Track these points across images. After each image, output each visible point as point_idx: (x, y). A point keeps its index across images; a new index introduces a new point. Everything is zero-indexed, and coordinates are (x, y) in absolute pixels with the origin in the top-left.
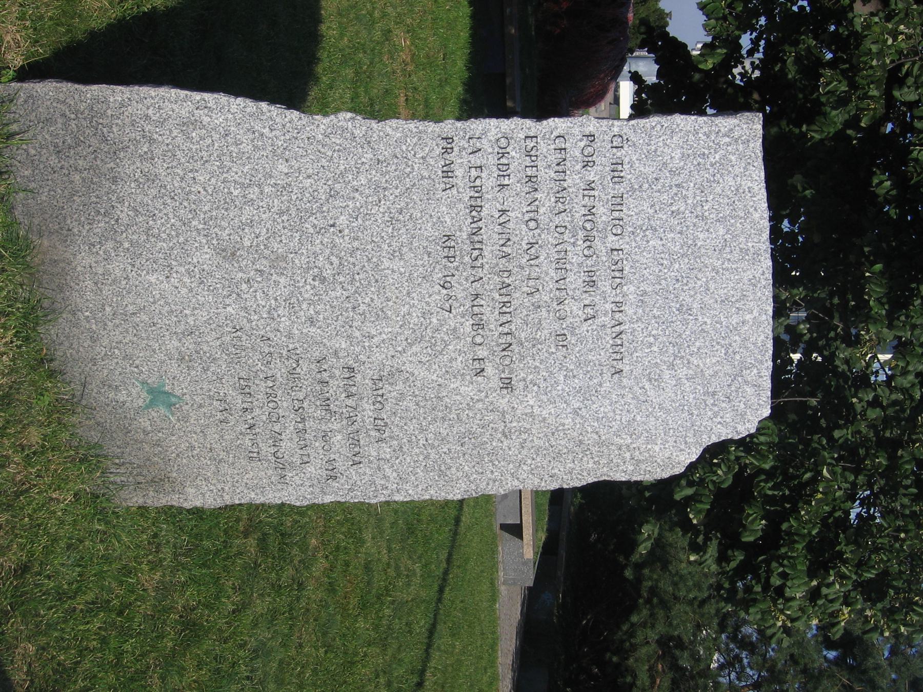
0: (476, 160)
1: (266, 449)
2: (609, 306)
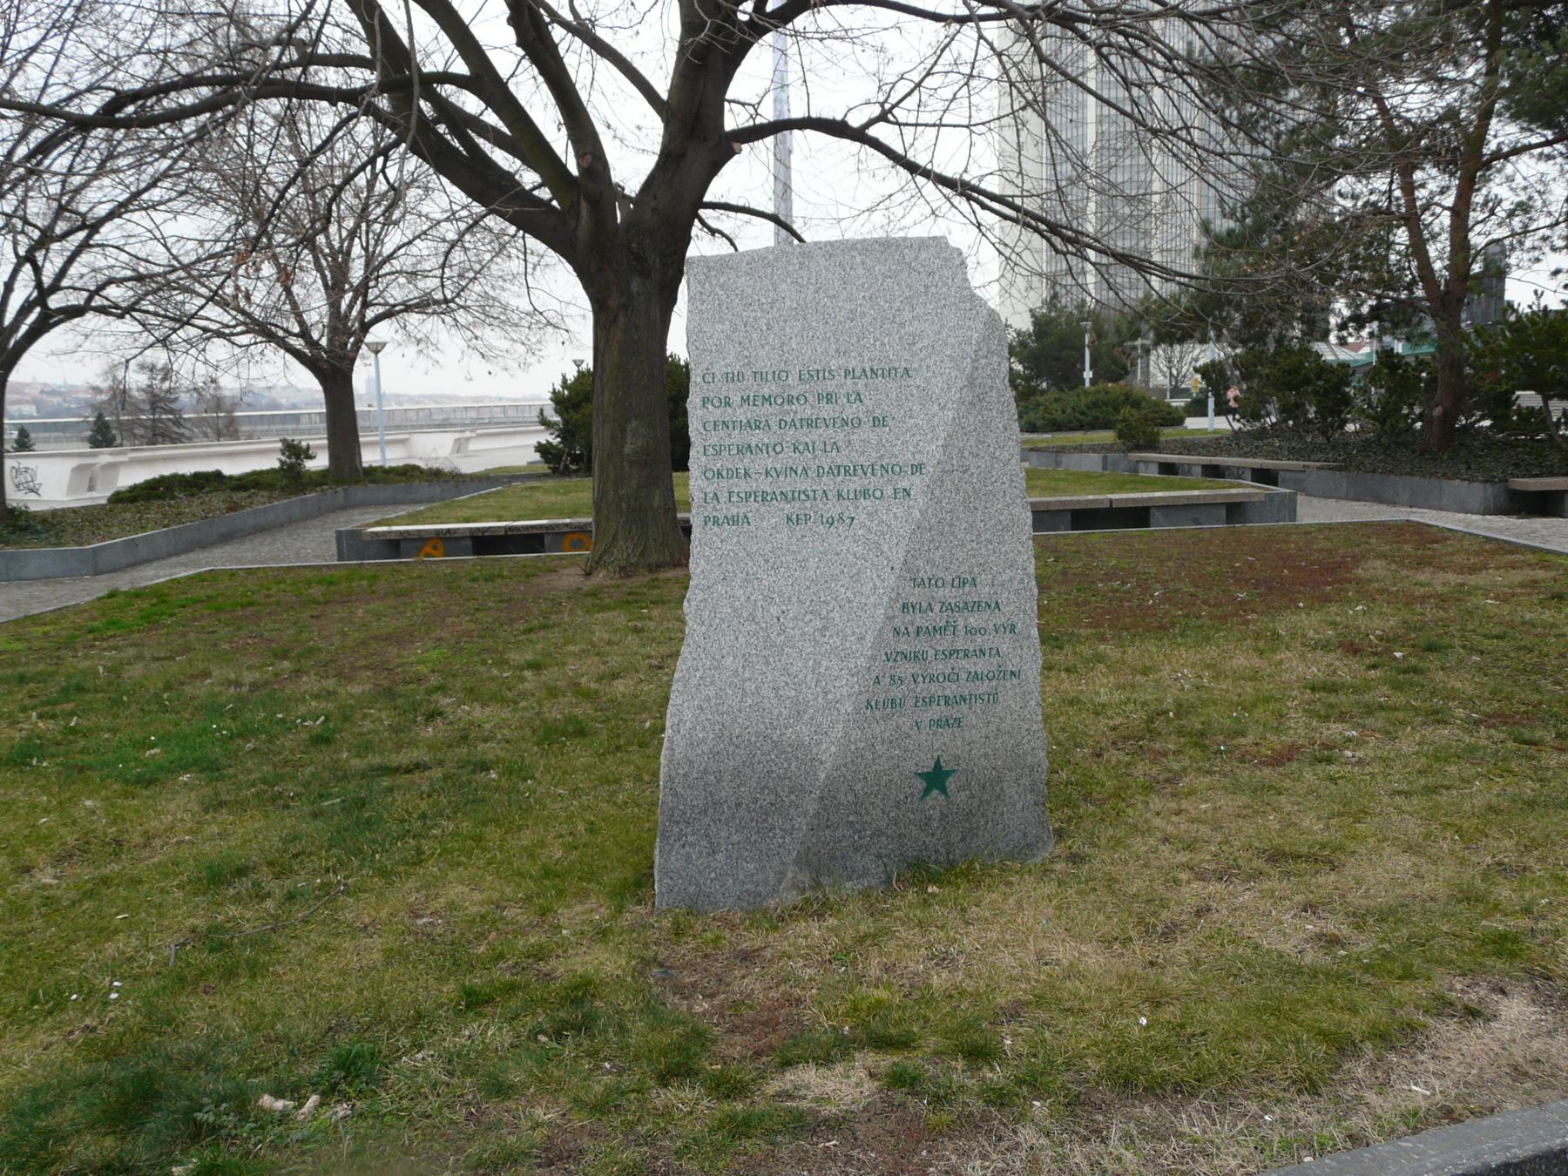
0: (723, 497)
1: (985, 687)
2: (849, 381)
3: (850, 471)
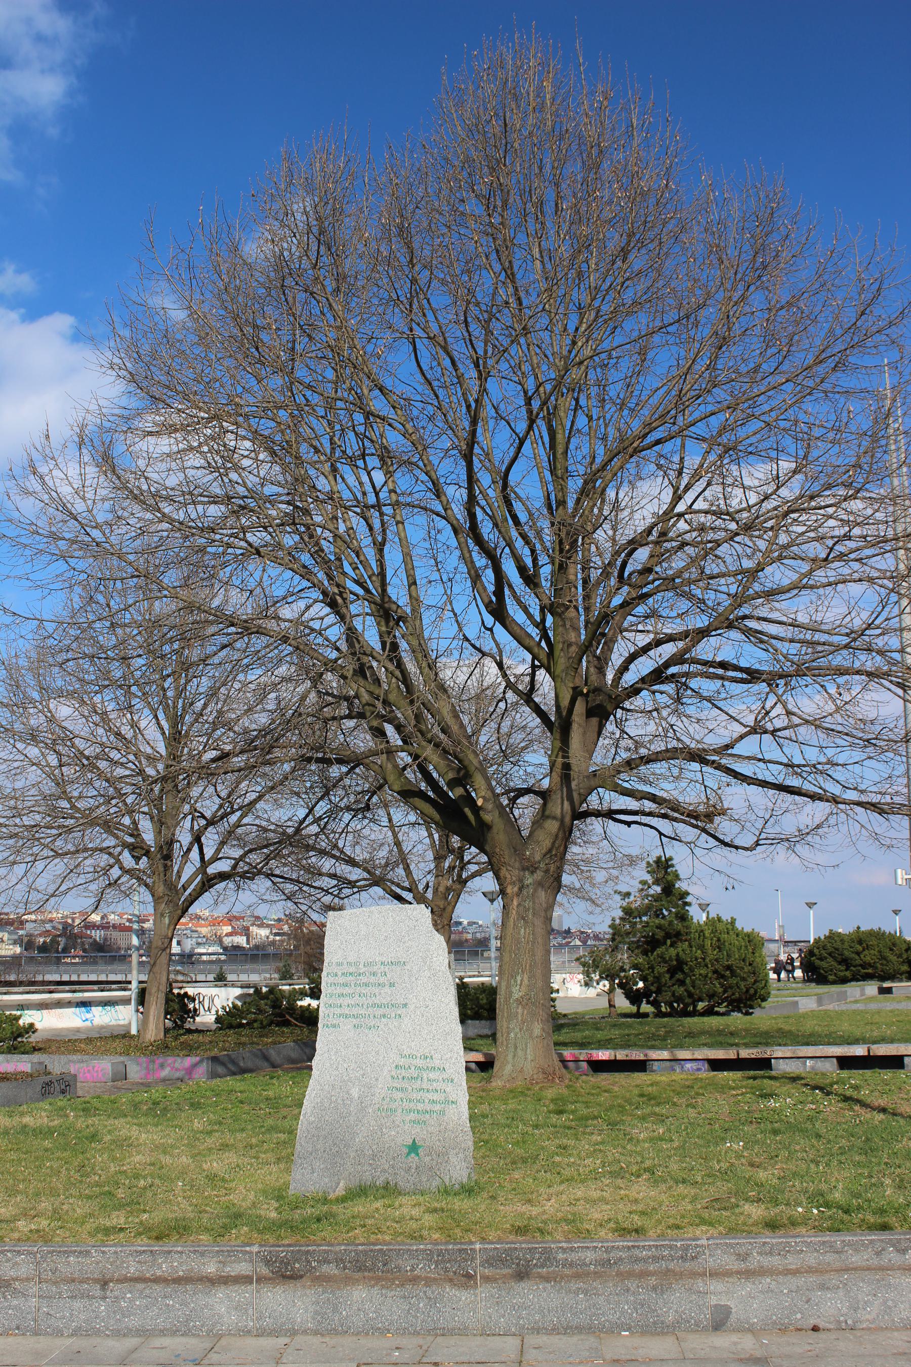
1: (437, 1107)
3: (380, 1006)
